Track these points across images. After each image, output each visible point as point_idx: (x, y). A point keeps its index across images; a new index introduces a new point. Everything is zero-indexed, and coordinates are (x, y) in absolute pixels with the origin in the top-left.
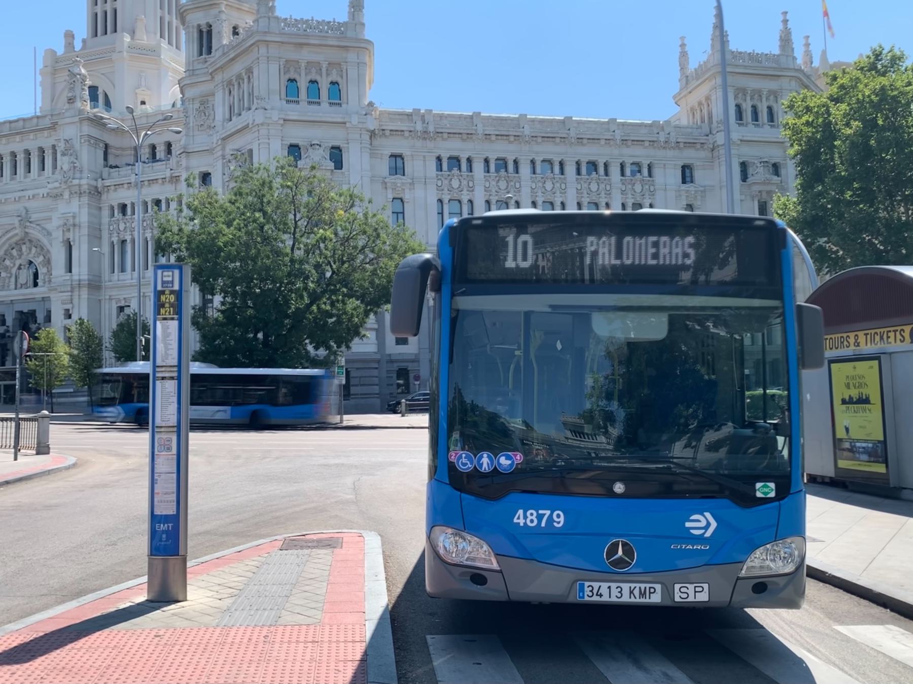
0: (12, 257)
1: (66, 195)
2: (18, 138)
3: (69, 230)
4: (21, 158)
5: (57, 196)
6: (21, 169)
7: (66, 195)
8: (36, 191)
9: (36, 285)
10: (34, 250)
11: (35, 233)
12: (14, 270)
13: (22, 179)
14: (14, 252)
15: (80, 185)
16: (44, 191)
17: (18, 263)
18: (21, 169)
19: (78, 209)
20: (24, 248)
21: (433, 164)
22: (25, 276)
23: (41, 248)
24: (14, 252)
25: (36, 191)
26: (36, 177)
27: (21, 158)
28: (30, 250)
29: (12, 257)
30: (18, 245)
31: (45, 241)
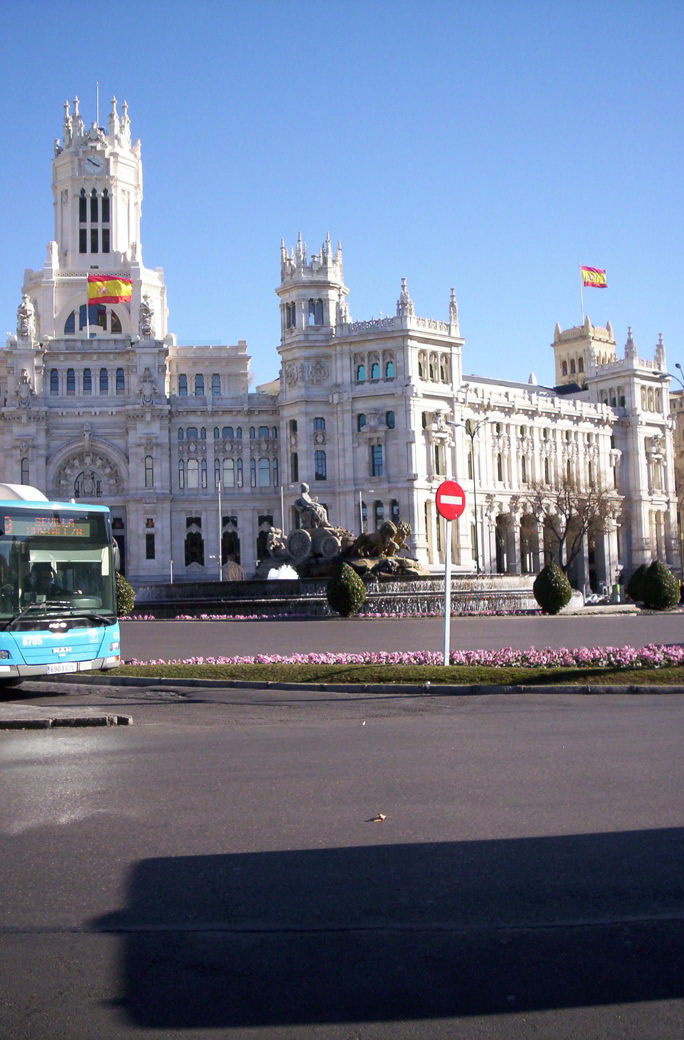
0: (103, 467)
1: (148, 417)
2: (79, 357)
4: (79, 376)
6: (79, 386)
7: (148, 417)
8: (105, 409)
10: (99, 462)
11: (102, 447)
12: (73, 479)
13: (82, 395)
14: (76, 463)
16: (115, 410)
17: (77, 472)
18: (79, 386)
19: (156, 429)
20: (88, 460)
23: (107, 462)
25: (105, 409)
26: (98, 394)
27: (79, 376)
28: (94, 461)
30: (80, 456)
31: (115, 457)
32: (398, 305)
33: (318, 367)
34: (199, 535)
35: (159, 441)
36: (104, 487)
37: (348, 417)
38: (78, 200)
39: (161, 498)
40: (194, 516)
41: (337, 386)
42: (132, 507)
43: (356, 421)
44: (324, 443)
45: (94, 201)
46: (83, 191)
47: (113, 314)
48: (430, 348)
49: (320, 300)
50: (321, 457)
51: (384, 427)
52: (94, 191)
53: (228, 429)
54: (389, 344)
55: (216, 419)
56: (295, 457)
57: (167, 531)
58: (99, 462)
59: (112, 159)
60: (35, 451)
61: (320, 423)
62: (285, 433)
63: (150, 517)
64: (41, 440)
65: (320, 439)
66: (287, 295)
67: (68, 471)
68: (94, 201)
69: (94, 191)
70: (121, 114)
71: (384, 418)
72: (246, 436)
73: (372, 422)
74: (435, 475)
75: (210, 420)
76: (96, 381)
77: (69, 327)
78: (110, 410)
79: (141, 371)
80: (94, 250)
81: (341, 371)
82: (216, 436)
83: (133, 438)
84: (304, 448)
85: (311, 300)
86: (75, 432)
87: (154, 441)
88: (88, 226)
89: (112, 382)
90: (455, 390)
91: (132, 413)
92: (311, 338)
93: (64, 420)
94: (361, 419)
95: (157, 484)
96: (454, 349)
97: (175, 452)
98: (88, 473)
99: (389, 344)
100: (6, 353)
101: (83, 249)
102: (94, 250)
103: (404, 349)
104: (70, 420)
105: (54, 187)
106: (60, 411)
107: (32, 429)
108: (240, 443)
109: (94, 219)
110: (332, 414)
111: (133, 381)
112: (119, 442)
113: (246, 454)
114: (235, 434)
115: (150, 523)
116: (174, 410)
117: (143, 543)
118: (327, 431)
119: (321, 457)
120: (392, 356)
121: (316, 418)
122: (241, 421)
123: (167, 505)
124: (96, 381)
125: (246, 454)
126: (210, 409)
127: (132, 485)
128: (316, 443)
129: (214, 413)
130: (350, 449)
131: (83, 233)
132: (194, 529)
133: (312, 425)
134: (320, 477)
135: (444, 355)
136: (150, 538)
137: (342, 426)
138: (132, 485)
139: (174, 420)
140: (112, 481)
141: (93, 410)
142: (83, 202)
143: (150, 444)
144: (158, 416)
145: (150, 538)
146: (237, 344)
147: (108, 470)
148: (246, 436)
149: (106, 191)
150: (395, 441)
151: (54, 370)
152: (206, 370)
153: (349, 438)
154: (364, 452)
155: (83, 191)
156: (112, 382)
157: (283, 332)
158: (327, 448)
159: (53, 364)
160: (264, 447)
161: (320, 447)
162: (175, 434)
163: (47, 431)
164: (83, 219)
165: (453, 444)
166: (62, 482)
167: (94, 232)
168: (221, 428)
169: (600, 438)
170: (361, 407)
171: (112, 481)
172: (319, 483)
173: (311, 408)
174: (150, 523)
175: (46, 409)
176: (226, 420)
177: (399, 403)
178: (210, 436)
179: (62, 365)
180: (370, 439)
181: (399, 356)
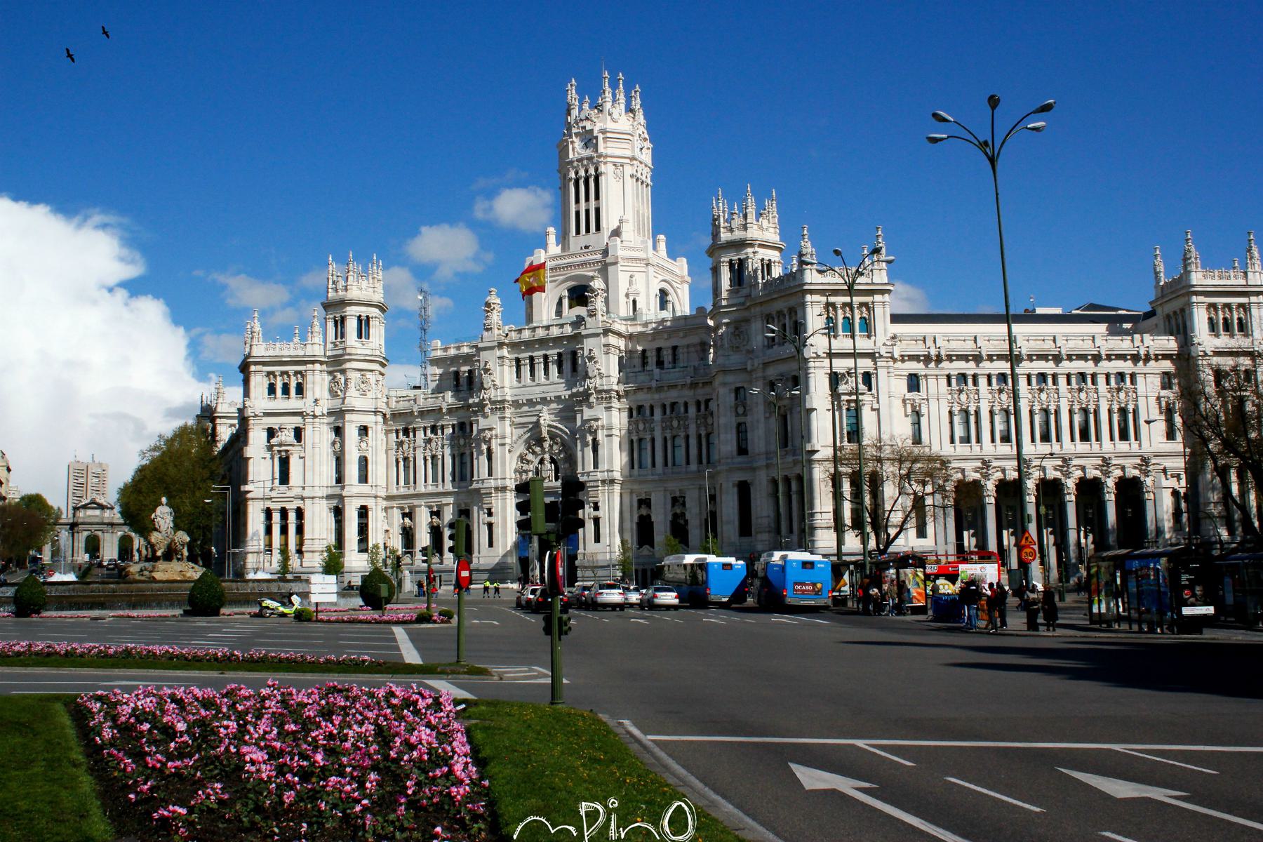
34: (649, 516)
40: (643, 497)
41: (750, 352)
44: (745, 414)
50: (741, 430)
55: (663, 395)
59: (601, 137)
65: (741, 410)
70: (614, 86)
72: (692, 410)
75: (656, 396)
77: (559, 313)
79: (586, 353)
80: (588, 230)
82: (665, 413)
90: (879, 344)
96: (878, 298)
101: (578, 232)
102: (588, 230)
103: (803, 305)
108: (686, 418)
113: (692, 430)
122: (688, 395)
125: (692, 430)
128: (737, 415)
130: (762, 419)
132: (644, 512)
133: (733, 395)
140: (567, 465)
152: (665, 344)
154: (774, 424)
158: (748, 419)
161: (741, 419)
165: (876, 406)
167: (587, 212)
169: (1140, 379)
171: (567, 465)
172: (740, 459)
173: (730, 378)
176: (671, 396)
178: (658, 414)
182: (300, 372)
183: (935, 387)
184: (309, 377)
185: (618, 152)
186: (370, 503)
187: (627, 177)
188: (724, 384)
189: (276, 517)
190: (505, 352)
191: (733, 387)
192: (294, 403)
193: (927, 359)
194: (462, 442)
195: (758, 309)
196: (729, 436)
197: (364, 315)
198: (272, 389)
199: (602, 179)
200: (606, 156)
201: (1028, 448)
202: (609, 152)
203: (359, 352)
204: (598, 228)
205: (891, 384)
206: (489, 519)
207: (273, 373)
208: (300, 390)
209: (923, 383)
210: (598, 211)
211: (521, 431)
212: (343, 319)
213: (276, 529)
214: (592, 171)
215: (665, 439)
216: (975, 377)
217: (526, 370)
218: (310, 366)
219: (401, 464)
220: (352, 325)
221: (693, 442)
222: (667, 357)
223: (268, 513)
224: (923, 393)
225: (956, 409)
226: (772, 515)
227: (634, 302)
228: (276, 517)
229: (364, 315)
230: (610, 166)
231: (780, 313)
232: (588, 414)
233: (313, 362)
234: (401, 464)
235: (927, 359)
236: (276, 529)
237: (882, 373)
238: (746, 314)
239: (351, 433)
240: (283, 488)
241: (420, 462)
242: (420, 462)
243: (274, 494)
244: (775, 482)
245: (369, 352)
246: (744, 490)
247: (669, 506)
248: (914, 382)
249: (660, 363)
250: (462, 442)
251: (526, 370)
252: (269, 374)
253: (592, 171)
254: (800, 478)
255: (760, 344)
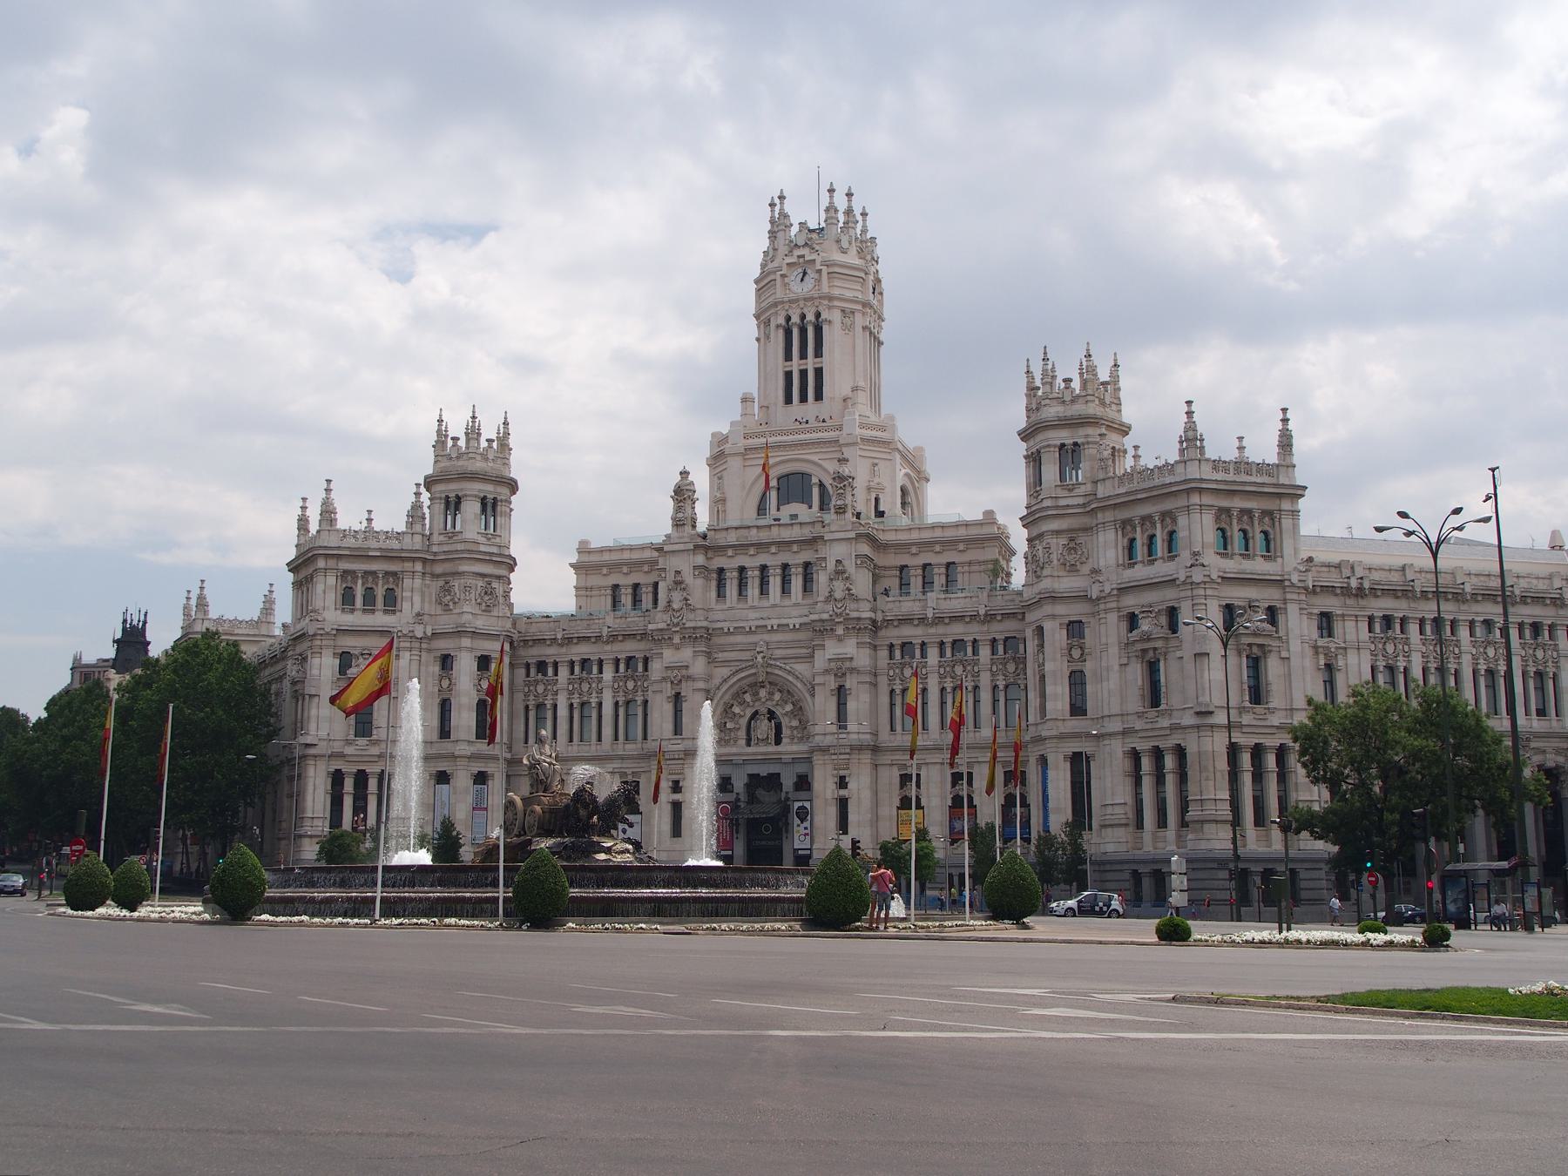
1: (840, 631)
3: (844, 674)
5: (821, 630)
6: (753, 590)
7: (840, 631)
9: (778, 741)
10: (777, 696)
15: (859, 619)
16: (798, 621)
18: (753, 590)
20: (763, 693)
21: (1364, 626)
22: (764, 728)
24: (748, 697)
25: (784, 621)
29: (742, 703)
30: (755, 686)
32: (1181, 442)
33: (1072, 545)
35: (854, 664)
36: (785, 732)
37: (1112, 618)
38: (781, 332)
39: (858, 748)
41: (1095, 571)
42: (818, 759)
43: (1124, 625)
44: (1082, 659)
45: (803, 331)
46: (788, 319)
47: (821, 485)
48: (1238, 503)
49: (1076, 444)
50: (1077, 681)
51: (1165, 632)
52: (803, 317)
53: (957, 644)
54: (1168, 505)
55: (941, 630)
56: (1043, 678)
57: (866, 795)
58: (777, 696)
60: (690, 683)
61: (1075, 629)
62: (1031, 646)
63: (842, 773)
64: (699, 666)
65: (1076, 653)
66: (1031, 442)
67: (736, 710)
68: (803, 331)
69: (803, 317)
71: (1164, 620)
72: (985, 652)
73: (1145, 626)
74: (1247, 704)
75: (932, 630)
76: (775, 583)
77: (761, 509)
78: (791, 622)
79: (831, 565)
80: (803, 399)
81: (1106, 549)
82: (942, 654)
83: (820, 661)
84: (1056, 667)
85: (1063, 445)
86: (746, 655)
87: (847, 664)
88: (796, 365)
89: (797, 583)
91: (818, 626)
92: (1062, 502)
93: (732, 639)
94: (1132, 621)
95: (852, 726)
97: (883, 681)
98: (763, 710)
99: (1168, 505)
100: (660, 549)
101: (788, 400)
102: (803, 399)
104: (739, 639)
105: (757, 317)
106: (725, 625)
107: (686, 654)
108: (976, 663)
109: (803, 356)
110: (1093, 614)
111: (822, 579)
112: (801, 668)
113: (985, 680)
114: (970, 650)
115: (842, 783)
116: (879, 617)
117: (833, 811)
118: (1089, 640)
119: (1077, 681)
120: (1174, 521)
121: (1071, 622)
123: (866, 757)
124: (775, 583)
125: (985, 680)
126: (930, 615)
127: (818, 729)
129: (939, 620)
130: (1116, 667)
131: (788, 376)
134: (1078, 709)
135: (1265, 513)
136: (843, 804)
137: (1107, 633)
138: (818, 729)
139: (882, 633)
141: (768, 623)
142: (788, 333)
143: (841, 669)
144: (854, 627)
145: (843, 804)
146: (980, 517)
147: (789, 707)
148: (985, 652)
149: (818, 315)
150: (1179, 654)
151: (721, 571)
153: (1114, 650)
154: (1137, 672)
155: (788, 319)
156: (797, 583)
157: (1030, 496)
158: (1088, 667)
159: (719, 562)
160: (1011, 667)
162: (884, 653)
163: (708, 654)
164: (788, 356)
165: (1284, 654)
166: (729, 725)
167: (803, 373)
168: (948, 640)
170: (1131, 602)
171: (795, 723)
173: (1060, 609)
174: (842, 783)
175: (705, 624)
176: (957, 630)
177: (1183, 594)
179: (730, 563)
180: (1144, 651)
181: (1182, 521)
182: (394, 574)
183: (1351, 631)
184: (407, 582)
185: (849, 294)
186: (490, 768)
187: (859, 329)
188: (1053, 617)
189: (349, 785)
190: (700, 559)
191: (1066, 621)
192: (380, 619)
193: (1346, 591)
194: (630, 685)
195: (1109, 516)
196: (1059, 689)
197: (490, 496)
198: (347, 599)
199: (825, 328)
200: (831, 298)
201: (1521, 720)
202: (836, 292)
203: (482, 548)
204: (819, 396)
205: (1298, 626)
206: (677, 797)
207: (353, 573)
208: (391, 602)
209: (1338, 627)
210: (819, 372)
211: (725, 672)
212: (459, 499)
213: (348, 802)
214: (810, 317)
215: (943, 690)
216: (1403, 621)
217: (731, 589)
218: (408, 566)
219: (532, 714)
220: (471, 508)
221: (985, 696)
222: (939, 580)
223: (337, 778)
224: (1338, 640)
225: (1381, 664)
226: (1129, 799)
227: (877, 500)
228: (349, 785)
229: (490, 496)
230: (836, 316)
231: (1147, 519)
232: (832, 649)
233: (413, 560)
234: (532, 714)
235: (1346, 591)
236: (348, 802)
237: (1292, 609)
238: (1086, 521)
239: (465, 667)
240: (362, 741)
241: (563, 712)
242: (563, 712)
243: (349, 750)
244: (1135, 756)
245: (495, 550)
246: (1078, 762)
247: (949, 785)
248: (1326, 622)
249: (927, 584)
250: (630, 685)
251: (731, 589)
252: (345, 572)
253: (810, 317)
254: (1180, 752)
255: (1112, 562)
